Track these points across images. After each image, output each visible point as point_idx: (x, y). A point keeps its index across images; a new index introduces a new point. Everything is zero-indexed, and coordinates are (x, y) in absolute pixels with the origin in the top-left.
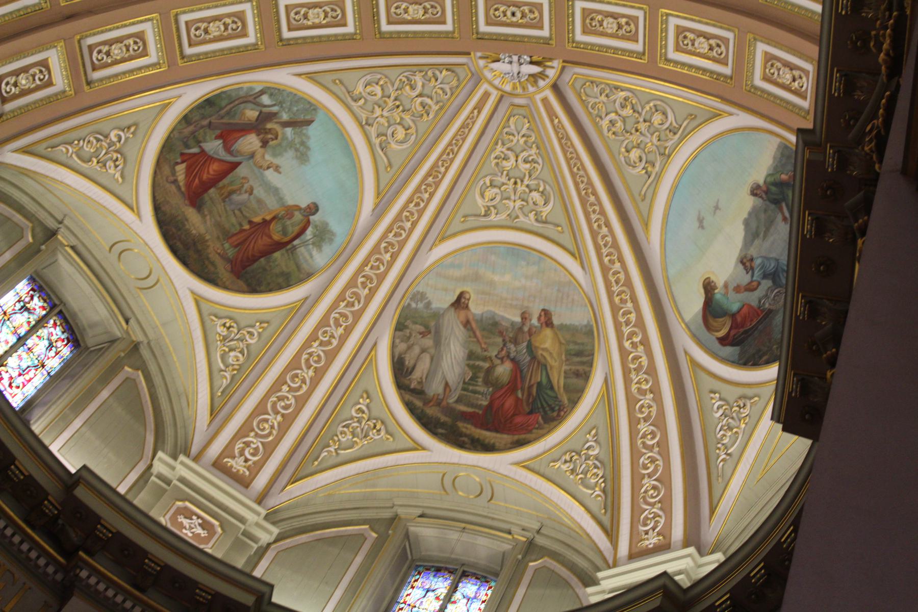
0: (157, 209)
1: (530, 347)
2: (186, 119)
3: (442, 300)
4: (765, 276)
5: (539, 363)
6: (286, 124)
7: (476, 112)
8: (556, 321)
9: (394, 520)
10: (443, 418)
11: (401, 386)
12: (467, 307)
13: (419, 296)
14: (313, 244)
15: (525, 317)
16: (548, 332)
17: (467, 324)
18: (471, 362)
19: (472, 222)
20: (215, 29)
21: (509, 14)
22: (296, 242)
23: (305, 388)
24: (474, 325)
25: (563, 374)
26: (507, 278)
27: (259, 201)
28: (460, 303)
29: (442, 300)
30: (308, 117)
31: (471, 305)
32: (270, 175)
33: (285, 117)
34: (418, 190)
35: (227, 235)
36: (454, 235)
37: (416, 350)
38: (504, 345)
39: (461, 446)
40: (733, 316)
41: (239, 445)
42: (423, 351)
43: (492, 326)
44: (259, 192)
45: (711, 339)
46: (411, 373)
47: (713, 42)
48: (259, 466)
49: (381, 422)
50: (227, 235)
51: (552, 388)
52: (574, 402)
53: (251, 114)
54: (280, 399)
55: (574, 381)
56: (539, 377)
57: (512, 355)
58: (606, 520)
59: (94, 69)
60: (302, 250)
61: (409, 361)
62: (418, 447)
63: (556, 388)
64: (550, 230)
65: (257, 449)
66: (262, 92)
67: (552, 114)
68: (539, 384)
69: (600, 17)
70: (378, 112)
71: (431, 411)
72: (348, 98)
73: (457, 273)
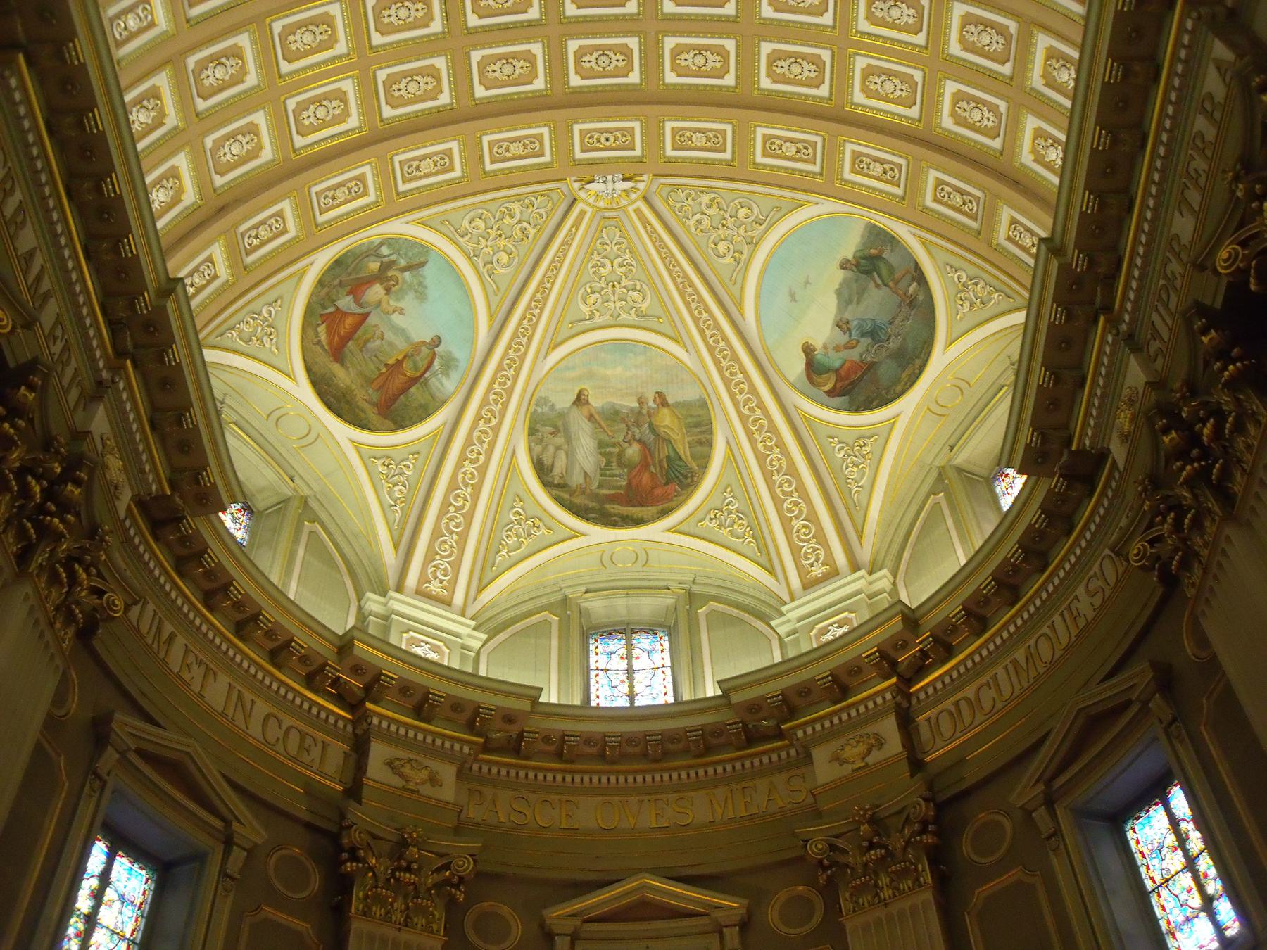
0: (309, 371)
1: (651, 427)
2: (321, 283)
3: (564, 401)
4: (863, 335)
5: (664, 440)
6: (404, 270)
7: (574, 229)
8: (670, 400)
9: (565, 601)
10: (592, 504)
11: (547, 484)
12: (587, 403)
13: (543, 401)
14: (442, 373)
15: (641, 401)
16: (665, 411)
17: (591, 417)
18: (603, 450)
19: (579, 327)
20: (341, 194)
21: (603, 140)
22: (426, 375)
23: (468, 504)
24: (597, 417)
25: (687, 446)
26: (619, 370)
27: (391, 344)
28: (580, 400)
29: (564, 401)
30: (422, 259)
31: (591, 401)
32: (396, 318)
33: (403, 263)
34: (528, 307)
35: (369, 382)
36: (562, 342)
37: (551, 449)
38: (629, 429)
39: (614, 525)
40: (837, 371)
41: (430, 570)
42: (558, 448)
43: (614, 415)
44: (389, 335)
45: (819, 392)
46: (551, 471)
47: (887, 166)
48: (454, 582)
49: (536, 519)
50: (369, 382)
51: (680, 458)
52: (704, 467)
53: (374, 266)
54: (451, 519)
55: (699, 448)
56: (665, 452)
57: (637, 437)
58: (763, 561)
59: (248, 254)
60: (433, 382)
61: (547, 461)
62: (577, 534)
63: (683, 457)
64: (650, 322)
65: (445, 569)
66: (381, 244)
67: (645, 222)
68: (668, 458)
69: (688, 134)
70: (483, 242)
71: (578, 500)
72: (456, 235)
73: (573, 374)
